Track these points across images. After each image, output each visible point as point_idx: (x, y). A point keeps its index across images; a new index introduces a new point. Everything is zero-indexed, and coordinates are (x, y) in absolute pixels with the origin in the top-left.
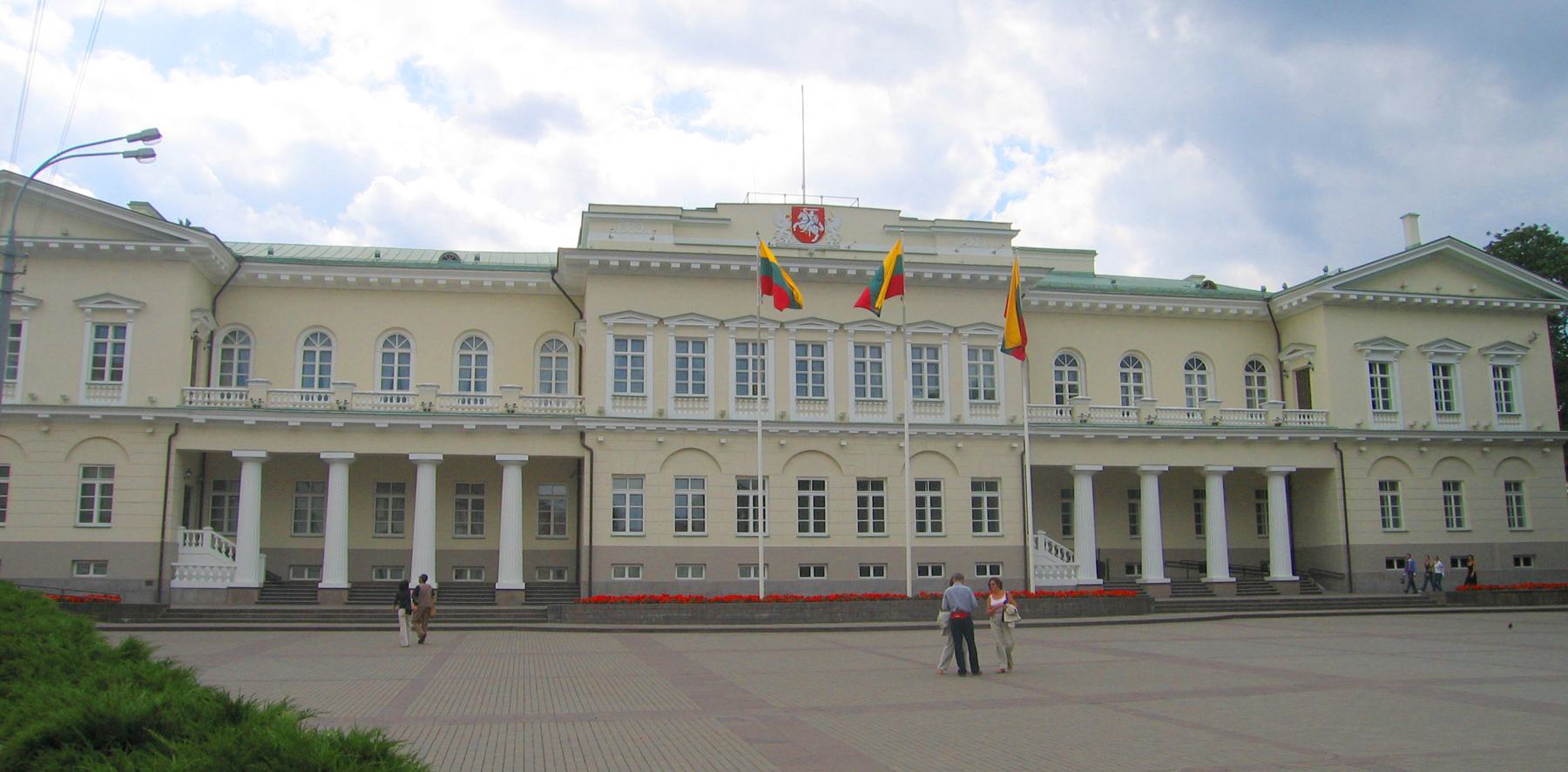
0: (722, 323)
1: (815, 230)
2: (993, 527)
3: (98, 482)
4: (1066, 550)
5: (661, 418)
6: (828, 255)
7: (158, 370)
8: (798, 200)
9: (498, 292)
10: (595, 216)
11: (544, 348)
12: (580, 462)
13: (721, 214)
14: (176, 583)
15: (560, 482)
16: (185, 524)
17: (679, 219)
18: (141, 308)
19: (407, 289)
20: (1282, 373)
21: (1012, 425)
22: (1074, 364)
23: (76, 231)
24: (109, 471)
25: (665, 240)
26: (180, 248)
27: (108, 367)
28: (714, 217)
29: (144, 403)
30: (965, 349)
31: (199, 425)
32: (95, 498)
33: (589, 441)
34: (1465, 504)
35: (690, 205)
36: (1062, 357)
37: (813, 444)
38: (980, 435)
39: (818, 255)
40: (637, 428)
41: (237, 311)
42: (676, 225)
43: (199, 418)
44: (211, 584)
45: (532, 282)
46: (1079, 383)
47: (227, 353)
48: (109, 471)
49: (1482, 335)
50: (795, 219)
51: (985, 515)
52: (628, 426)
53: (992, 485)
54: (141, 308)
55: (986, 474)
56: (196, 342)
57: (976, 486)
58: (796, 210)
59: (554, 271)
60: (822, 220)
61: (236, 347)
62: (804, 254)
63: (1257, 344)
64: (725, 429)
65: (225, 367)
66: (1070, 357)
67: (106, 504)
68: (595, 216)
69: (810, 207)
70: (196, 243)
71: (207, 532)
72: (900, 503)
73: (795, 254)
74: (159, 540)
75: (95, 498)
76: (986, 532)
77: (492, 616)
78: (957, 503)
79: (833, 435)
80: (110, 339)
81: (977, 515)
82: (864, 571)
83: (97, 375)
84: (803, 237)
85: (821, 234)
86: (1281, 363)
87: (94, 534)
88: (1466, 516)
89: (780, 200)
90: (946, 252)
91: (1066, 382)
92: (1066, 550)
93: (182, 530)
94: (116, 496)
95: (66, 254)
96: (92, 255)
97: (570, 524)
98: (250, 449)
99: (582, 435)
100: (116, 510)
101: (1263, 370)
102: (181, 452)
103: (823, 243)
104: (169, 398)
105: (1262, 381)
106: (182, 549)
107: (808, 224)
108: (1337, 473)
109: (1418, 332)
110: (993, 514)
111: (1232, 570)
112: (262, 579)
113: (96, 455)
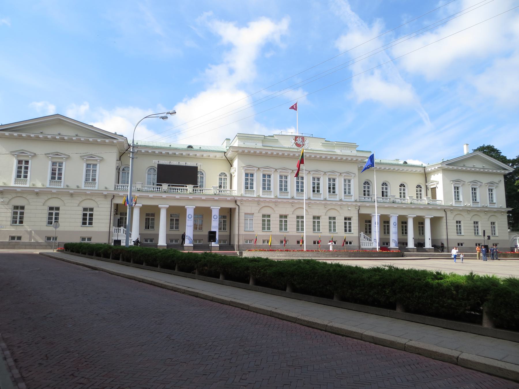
1: (301, 144)
2: (350, 231)
3: (88, 213)
10: (241, 137)
11: (220, 175)
12: (235, 209)
13: (276, 138)
18: (102, 160)
20: (427, 188)
21: (356, 201)
24: (92, 209)
25: (259, 145)
26: (115, 141)
27: (91, 178)
29: (103, 189)
30: (343, 179)
32: (87, 218)
34: (462, 228)
48: (92, 209)
49: (485, 180)
51: (347, 228)
54: (102, 160)
55: (348, 215)
57: (345, 219)
58: (296, 137)
63: (420, 181)
67: (91, 219)
69: (300, 137)
70: (120, 140)
71: (122, 228)
73: (296, 150)
74: (107, 230)
75: (87, 218)
81: (345, 227)
84: (297, 145)
85: (303, 145)
86: (426, 186)
87: (87, 229)
88: (462, 231)
90: (338, 151)
91: (366, 189)
93: (114, 228)
94: (94, 217)
95: (79, 142)
96: (87, 143)
97: (228, 227)
99: (236, 202)
100: (94, 221)
101: (421, 188)
105: (420, 191)
107: (299, 141)
108: (445, 218)
109: (468, 178)
111: (415, 245)
113: (88, 204)
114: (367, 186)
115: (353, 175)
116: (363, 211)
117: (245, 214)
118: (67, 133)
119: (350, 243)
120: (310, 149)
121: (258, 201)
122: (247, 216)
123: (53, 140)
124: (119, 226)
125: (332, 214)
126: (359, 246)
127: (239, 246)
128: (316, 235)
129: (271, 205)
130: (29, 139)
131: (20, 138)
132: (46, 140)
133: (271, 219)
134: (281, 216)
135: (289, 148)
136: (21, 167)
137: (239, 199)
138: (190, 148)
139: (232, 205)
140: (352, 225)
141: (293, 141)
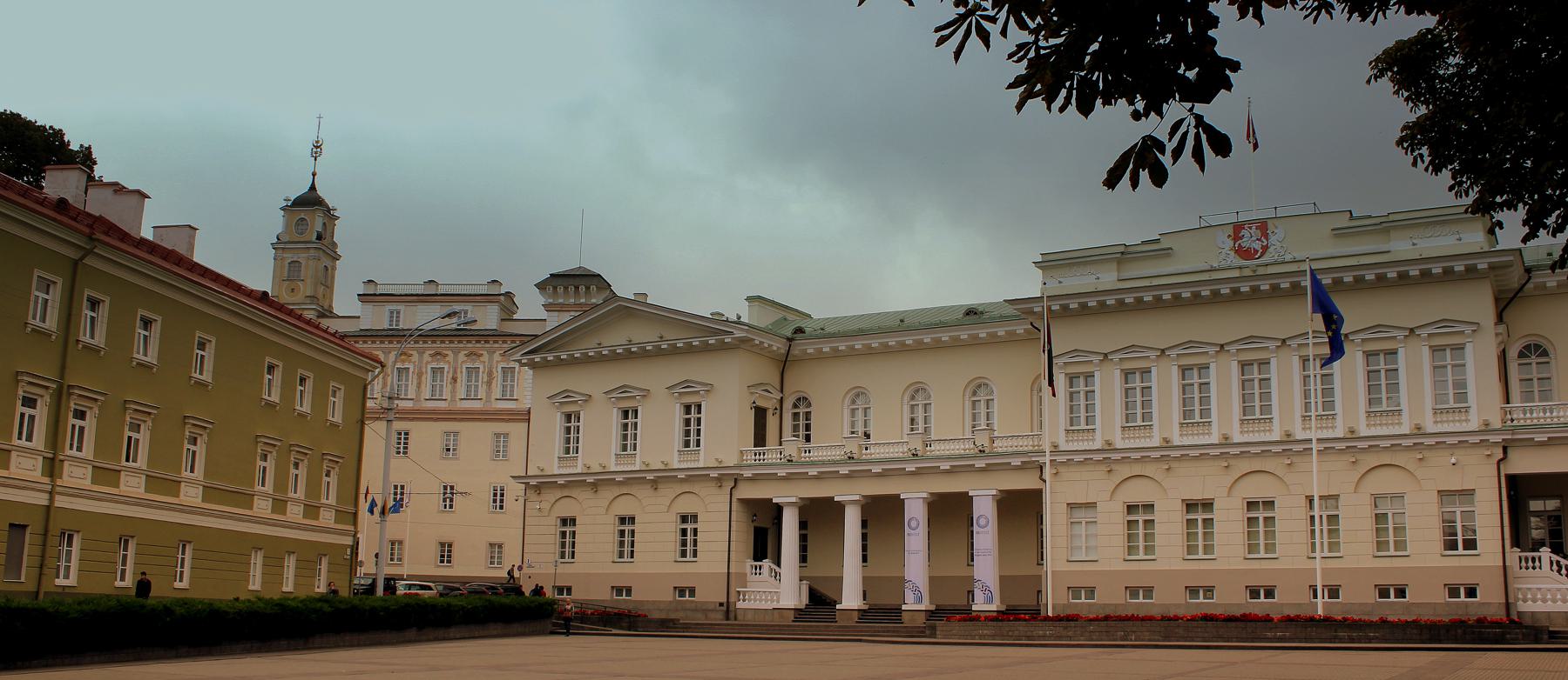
1: (1257, 245)
5: (1109, 447)
6: (1271, 270)
7: (726, 439)
9: (993, 341)
10: (1049, 264)
12: (1040, 491)
13: (1165, 244)
14: (740, 605)
16: (759, 554)
17: (1124, 255)
19: (920, 348)
21: (1486, 429)
23: (670, 334)
25: (1107, 278)
28: (1155, 250)
31: (749, 479)
35: (1133, 238)
37: (1257, 465)
38: (1441, 443)
39: (1261, 271)
40: (1087, 459)
41: (799, 382)
42: (1120, 262)
43: (747, 473)
44: (763, 605)
45: (1020, 330)
47: (796, 416)
50: (1236, 237)
52: (1450, 440)
54: (709, 388)
56: (760, 414)
58: (1238, 227)
60: (1266, 236)
61: (802, 410)
62: (1247, 272)
64: (1168, 455)
65: (796, 428)
68: (1049, 264)
69: (1251, 222)
70: (738, 334)
71: (767, 564)
72: (1229, 521)
73: (1236, 274)
76: (1461, 551)
77: (896, 633)
80: (693, 415)
83: (687, 444)
85: (1265, 248)
98: (786, 496)
102: (741, 501)
103: (1266, 259)
104: (731, 460)
106: (751, 578)
107: (1250, 240)
112: (805, 600)
115: (1468, 329)
116: (1526, 463)
117: (1072, 506)
118: (643, 335)
119: (1471, 592)
120: (1288, 258)
121: (1108, 458)
122: (1080, 515)
123: (614, 358)
124: (759, 554)
126: (1508, 605)
129: (1149, 469)
130: (573, 362)
131: (559, 363)
132: (600, 359)
133: (1156, 516)
134: (1190, 506)
136: (626, 425)
138: (972, 318)
139: (1025, 482)
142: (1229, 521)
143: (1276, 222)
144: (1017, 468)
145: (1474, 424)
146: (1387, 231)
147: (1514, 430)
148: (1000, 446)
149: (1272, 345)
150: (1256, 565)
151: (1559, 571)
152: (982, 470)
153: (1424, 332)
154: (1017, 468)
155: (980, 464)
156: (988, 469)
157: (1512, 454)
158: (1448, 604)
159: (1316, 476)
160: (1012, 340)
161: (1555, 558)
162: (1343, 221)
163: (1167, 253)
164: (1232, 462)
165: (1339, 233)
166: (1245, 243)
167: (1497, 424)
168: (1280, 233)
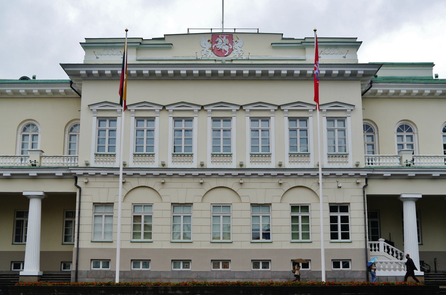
0: (164, 107)
1: (226, 48)
2: (346, 236)
4: (399, 251)
8: (220, 31)
9: (42, 96)
10: (89, 45)
12: (74, 194)
13: (167, 41)
15: (62, 208)
21: (357, 168)
22: (410, 130)
33: (78, 184)
36: (402, 126)
42: (138, 49)
45: (61, 90)
46: (415, 142)
51: (339, 228)
53: (344, 208)
55: (339, 200)
57: (333, 208)
59: (71, 83)
60: (232, 43)
64: (163, 174)
66: (407, 126)
69: (223, 33)
73: (213, 62)
76: (340, 239)
78: (320, 219)
79: (235, 176)
81: (334, 228)
82: (256, 264)
84: (219, 52)
85: (231, 50)
89: (210, 31)
92: (399, 251)
99: (76, 178)
103: (231, 57)
107: (222, 44)
110: (345, 228)
114: (405, 134)
116: (379, 189)
117: (96, 205)
119: (346, 265)
120: (244, 58)
122: (101, 210)
125: (300, 197)
127: (77, 272)
128: (262, 248)
129: (151, 183)
135: (197, 60)
137: (81, 172)
138: (25, 81)
140: (351, 222)
141: (209, 45)
142: (201, 216)
143: (238, 36)
144: (60, 178)
145: (351, 165)
146: (304, 48)
147: (373, 169)
148: (46, 162)
149: (234, 108)
150: (218, 247)
151: (388, 252)
152: (34, 178)
153: (325, 108)
154: (60, 178)
155: (33, 173)
156: (38, 177)
157: (370, 183)
158: (333, 272)
159: (260, 191)
160: (55, 96)
161: (387, 244)
162: (278, 40)
163: (169, 46)
164: (206, 180)
165: (275, 46)
166: (219, 46)
167: (362, 165)
168: (240, 43)
